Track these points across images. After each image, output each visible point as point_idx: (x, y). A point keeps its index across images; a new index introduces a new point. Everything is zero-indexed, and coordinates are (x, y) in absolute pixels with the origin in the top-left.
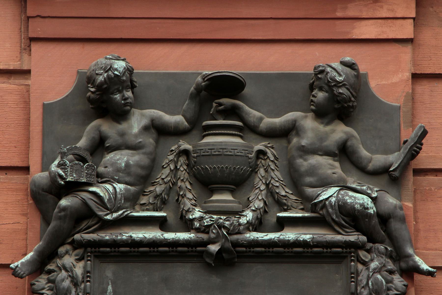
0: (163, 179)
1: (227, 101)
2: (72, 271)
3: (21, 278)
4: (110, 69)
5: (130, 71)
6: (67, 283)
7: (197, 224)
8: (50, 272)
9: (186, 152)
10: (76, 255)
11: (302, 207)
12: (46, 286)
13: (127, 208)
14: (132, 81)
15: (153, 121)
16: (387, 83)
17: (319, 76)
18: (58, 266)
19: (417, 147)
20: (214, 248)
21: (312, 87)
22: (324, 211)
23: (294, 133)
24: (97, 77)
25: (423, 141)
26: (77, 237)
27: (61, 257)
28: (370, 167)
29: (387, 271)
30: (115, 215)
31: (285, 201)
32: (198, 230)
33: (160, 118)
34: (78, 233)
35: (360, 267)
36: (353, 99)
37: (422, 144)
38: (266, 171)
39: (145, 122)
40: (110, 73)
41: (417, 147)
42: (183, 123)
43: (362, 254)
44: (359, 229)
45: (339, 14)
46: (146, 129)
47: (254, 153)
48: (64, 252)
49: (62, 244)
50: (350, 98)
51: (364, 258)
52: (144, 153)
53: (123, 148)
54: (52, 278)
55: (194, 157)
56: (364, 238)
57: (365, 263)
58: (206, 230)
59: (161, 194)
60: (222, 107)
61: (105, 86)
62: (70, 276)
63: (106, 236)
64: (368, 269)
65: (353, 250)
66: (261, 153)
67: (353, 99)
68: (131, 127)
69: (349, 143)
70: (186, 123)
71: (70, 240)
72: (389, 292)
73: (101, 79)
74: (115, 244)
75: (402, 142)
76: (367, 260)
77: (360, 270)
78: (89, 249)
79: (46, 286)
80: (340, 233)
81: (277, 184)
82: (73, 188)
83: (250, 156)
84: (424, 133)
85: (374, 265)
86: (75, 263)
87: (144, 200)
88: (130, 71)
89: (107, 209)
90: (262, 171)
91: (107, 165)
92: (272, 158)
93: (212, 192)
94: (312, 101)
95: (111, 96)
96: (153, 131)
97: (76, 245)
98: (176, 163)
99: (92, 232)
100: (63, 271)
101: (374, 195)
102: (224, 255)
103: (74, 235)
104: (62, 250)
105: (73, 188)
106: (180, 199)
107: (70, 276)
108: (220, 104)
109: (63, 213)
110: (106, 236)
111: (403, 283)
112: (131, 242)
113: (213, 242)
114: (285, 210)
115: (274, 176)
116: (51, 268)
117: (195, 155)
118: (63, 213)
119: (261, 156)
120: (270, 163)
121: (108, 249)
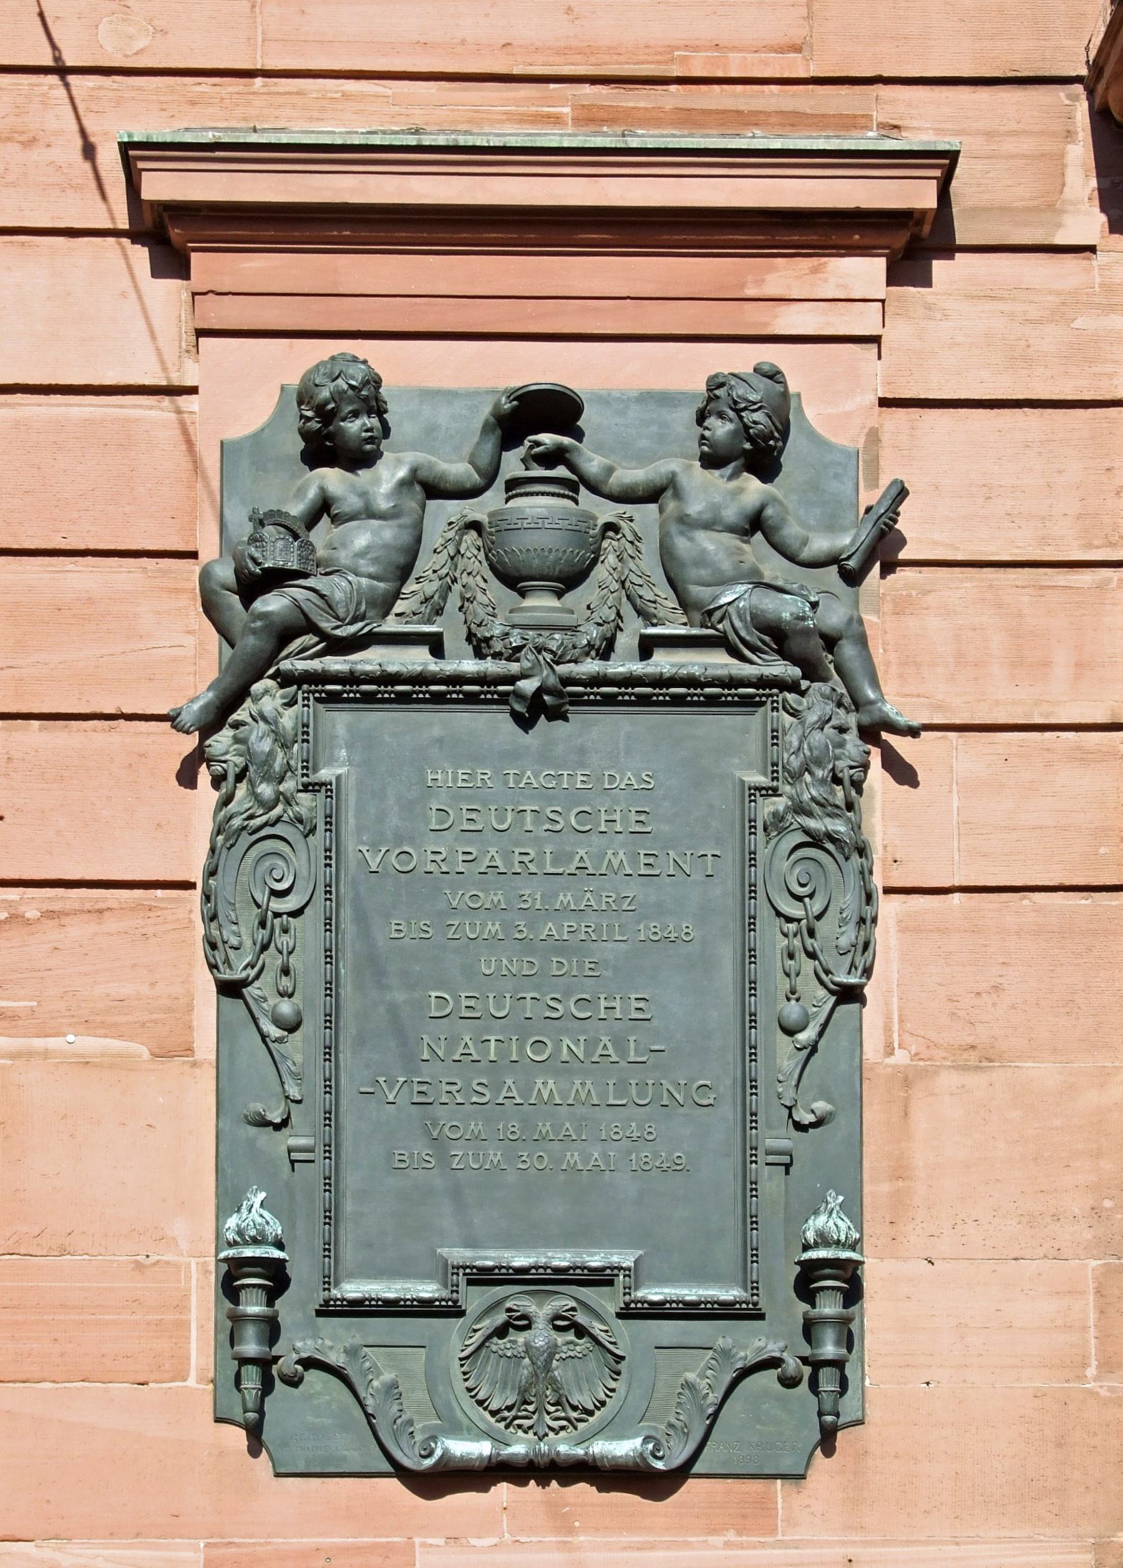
0: (435, 572)
1: (548, 439)
2: (276, 723)
3: (188, 732)
4: (339, 375)
5: (375, 382)
6: (266, 745)
7: (498, 646)
8: (236, 725)
9: (476, 526)
10: (283, 697)
11: (685, 620)
12: (232, 749)
13: (371, 618)
14: (377, 398)
15: (414, 471)
16: (834, 411)
17: (717, 392)
18: (251, 715)
19: (891, 519)
20: (528, 686)
21: (701, 417)
22: (726, 622)
23: (669, 493)
24: (317, 390)
25: (900, 509)
26: (285, 665)
27: (256, 700)
28: (805, 554)
29: (834, 728)
30: (352, 629)
31: (653, 610)
32: (497, 656)
33: (431, 467)
34: (287, 657)
35: (787, 719)
36: (776, 434)
37: (898, 514)
38: (620, 559)
39: (402, 473)
40: (340, 381)
41: (891, 519)
42: (470, 476)
43: (791, 697)
44: (784, 654)
45: (750, 292)
46: (404, 484)
47: (598, 528)
48: (261, 691)
49: (259, 677)
50: (772, 432)
51: (795, 706)
52: (400, 526)
53: (363, 516)
54: (241, 736)
55: (491, 534)
56: (796, 672)
57: (795, 713)
58: (514, 654)
59: (432, 597)
60: (541, 448)
61: (331, 406)
62: (273, 731)
63: (336, 664)
64: (802, 723)
65: (775, 691)
66: (611, 527)
67: (776, 434)
68: (377, 481)
69: (769, 512)
70: (476, 476)
71: (271, 671)
72: (837, 763)
73: (325, 394)
74: (351, 678)
75: (862, 511)
76: (800, 708)
77: (787, 726)
78: (305, 687)
79: (232, 749)
80: (751, 662)
81: (639, 581)
82: (276, 578)
83: (591, 532)
84: (902, 493)
85: (812, 718)
86: (281, 710)
87: (400, 606)
88: (375, 382)
89: (338, 618)
90: (611, 559)
91: (336, 545)
92: (630, 537)
93: (523, 594)
94: (703, 437)
95: (342, 424)
96: (418, 488)
97: (285, 680)
98: (459, 543)
99: (312, 657)
100: (261, 723)
101: (812, 599)
102: (546, 698)
103: (278, 663)
104: (257, 687)
105: (276, 578)
106: (466, 604)
107: (273, 731)
108: (538, 444)
109: (259, 624)
110: (336, 664)
111: (861, 749)
112: (380, 676)
113: (524, 676)
114: (654, 625)
115: (634, 568)
116: (239, 718)
117: (493, 530)
118: (259, 624)
119: (611, 534)
120: (628, 545)
121: (339, 687)
